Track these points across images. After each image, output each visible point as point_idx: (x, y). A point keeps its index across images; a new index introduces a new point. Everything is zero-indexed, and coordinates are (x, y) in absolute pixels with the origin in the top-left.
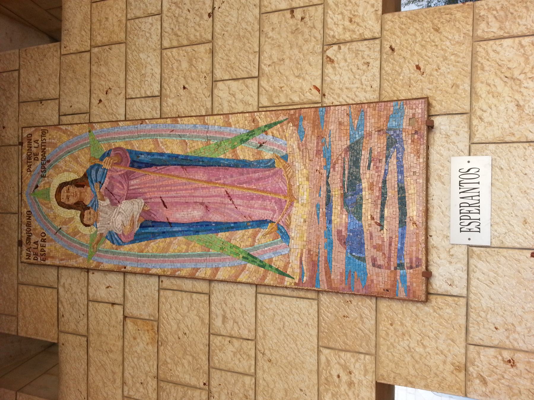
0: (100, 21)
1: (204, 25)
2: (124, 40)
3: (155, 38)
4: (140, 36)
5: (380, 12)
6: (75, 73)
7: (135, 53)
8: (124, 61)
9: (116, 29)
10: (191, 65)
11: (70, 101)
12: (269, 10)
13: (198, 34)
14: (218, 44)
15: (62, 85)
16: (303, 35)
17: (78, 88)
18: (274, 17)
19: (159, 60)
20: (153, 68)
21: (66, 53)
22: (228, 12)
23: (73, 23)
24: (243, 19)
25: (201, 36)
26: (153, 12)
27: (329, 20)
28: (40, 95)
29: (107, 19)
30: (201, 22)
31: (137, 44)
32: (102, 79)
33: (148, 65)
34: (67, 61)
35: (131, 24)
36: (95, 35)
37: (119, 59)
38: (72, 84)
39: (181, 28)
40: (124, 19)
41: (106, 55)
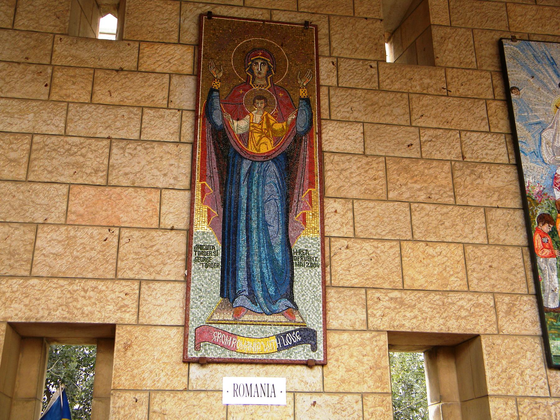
0: (74, 77)
1: (43, 175)
2: (51, 99)
3: (44, 129)
4: (50, 114)
5: (10, 320)
6: (32, 48)
7: (36, 109)
8: (31, 98)
9: (64, 92)
10: (11, 161)
11: (6, 41)
12: (39, 231)
13: (36, 168)
14: (22, 186)
15: (24, 33)
16: (8, 259)
17: (18, 50)
18: (31, 236)
19: (23, 131)
20: (18, 125)
21: (55, 40)
22: (47, 197)
23: (81, 49)
24: (37, 209)
25: (34, 171)
26: (68, 128)
27: (15, 281)
28: (21, 10)
29: (74, 84)
30: (46, 172)
31: (43, 111)
32: (20, 76)
33: (21, 120)
34: (47, 40)
35: (63, 106)
36: (63, 71)
37: (34, 92)
38: (23, 44)
39: (46, 153)
40: (70, 100)
41: (42, 80)
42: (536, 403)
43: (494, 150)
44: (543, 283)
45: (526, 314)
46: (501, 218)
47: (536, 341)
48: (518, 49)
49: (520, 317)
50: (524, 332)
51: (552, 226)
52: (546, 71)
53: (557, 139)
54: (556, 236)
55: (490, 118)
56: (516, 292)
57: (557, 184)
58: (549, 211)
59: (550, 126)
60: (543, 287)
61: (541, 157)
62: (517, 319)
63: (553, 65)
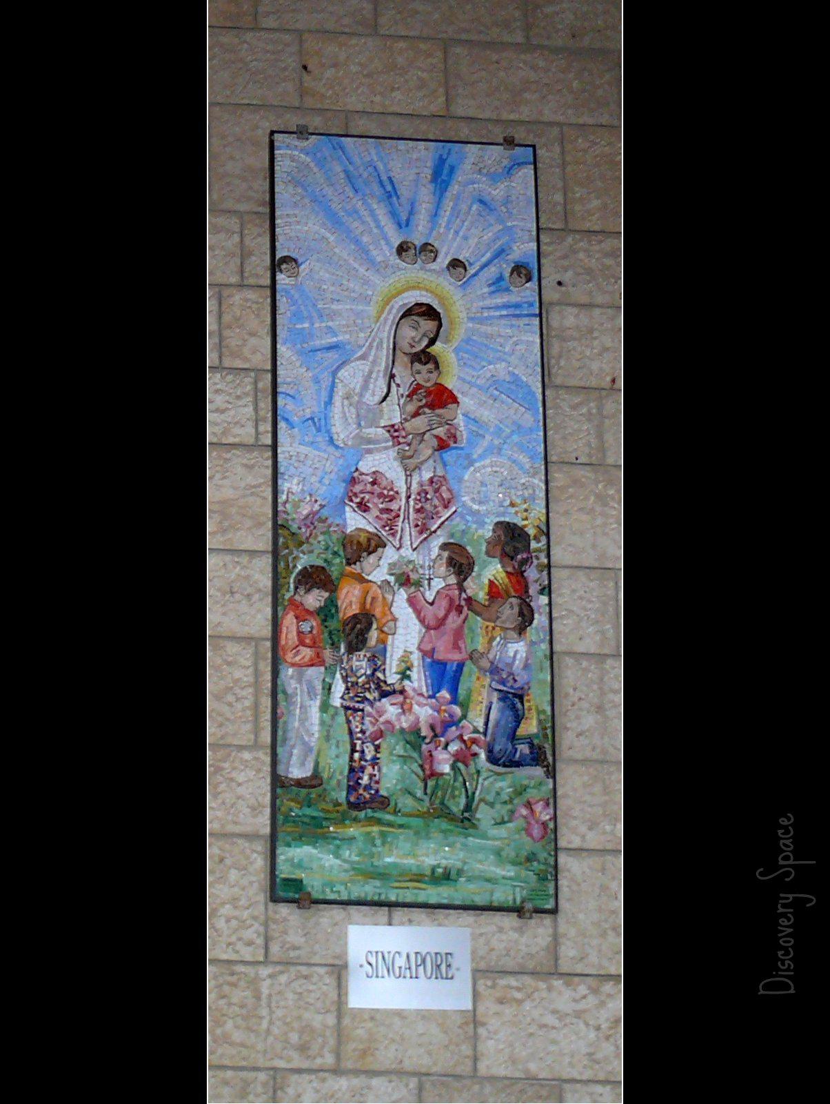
42: (233, 974)
43: (223, 411)
44: (285, 723)
45: (240, 790)
46: (219, 573)
47: (254, 847)
48: (308, 159)
49: (227, 795)
50: (231, 828)
51: (326, 595)
52: (372, 212)
53: (371, 386)
54: (333, 617)
55: (226, 333)
56: (229, 740)
57: (356, 495)
58: (326, 561)
59: (360, 353)
60: (284, 732)
61: (328, 431)
62: (220, 801)
63: (390, 197)
